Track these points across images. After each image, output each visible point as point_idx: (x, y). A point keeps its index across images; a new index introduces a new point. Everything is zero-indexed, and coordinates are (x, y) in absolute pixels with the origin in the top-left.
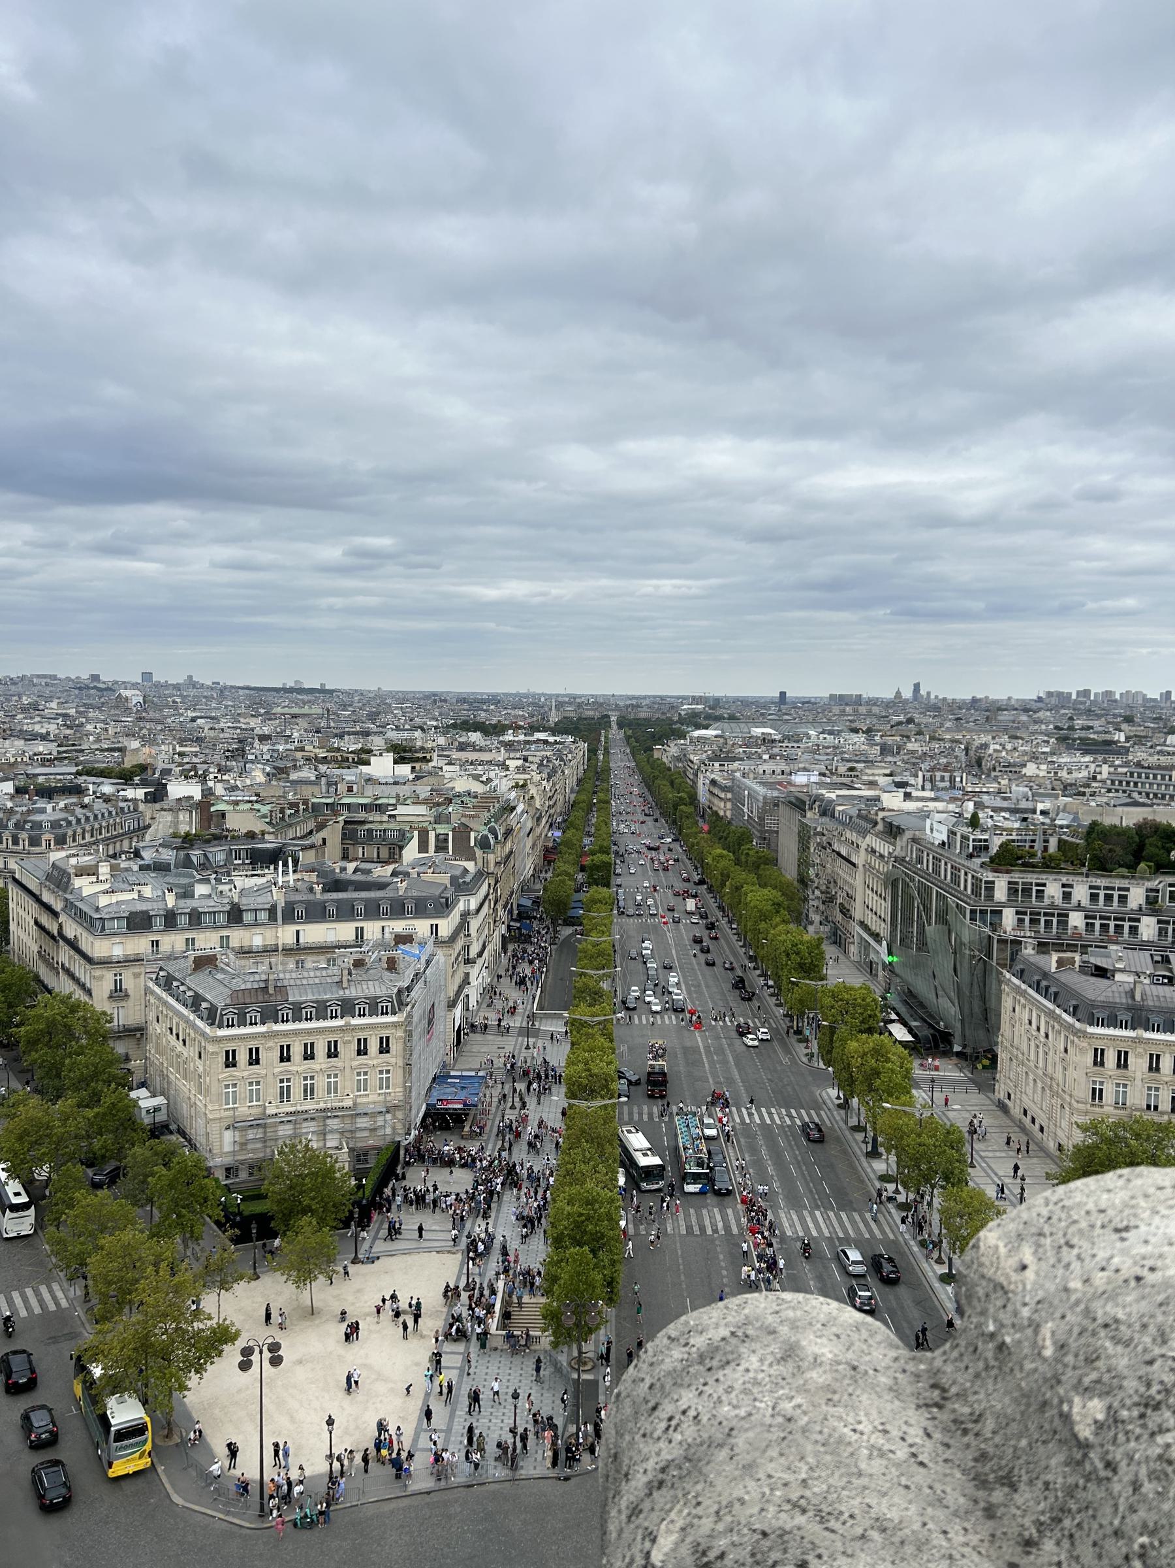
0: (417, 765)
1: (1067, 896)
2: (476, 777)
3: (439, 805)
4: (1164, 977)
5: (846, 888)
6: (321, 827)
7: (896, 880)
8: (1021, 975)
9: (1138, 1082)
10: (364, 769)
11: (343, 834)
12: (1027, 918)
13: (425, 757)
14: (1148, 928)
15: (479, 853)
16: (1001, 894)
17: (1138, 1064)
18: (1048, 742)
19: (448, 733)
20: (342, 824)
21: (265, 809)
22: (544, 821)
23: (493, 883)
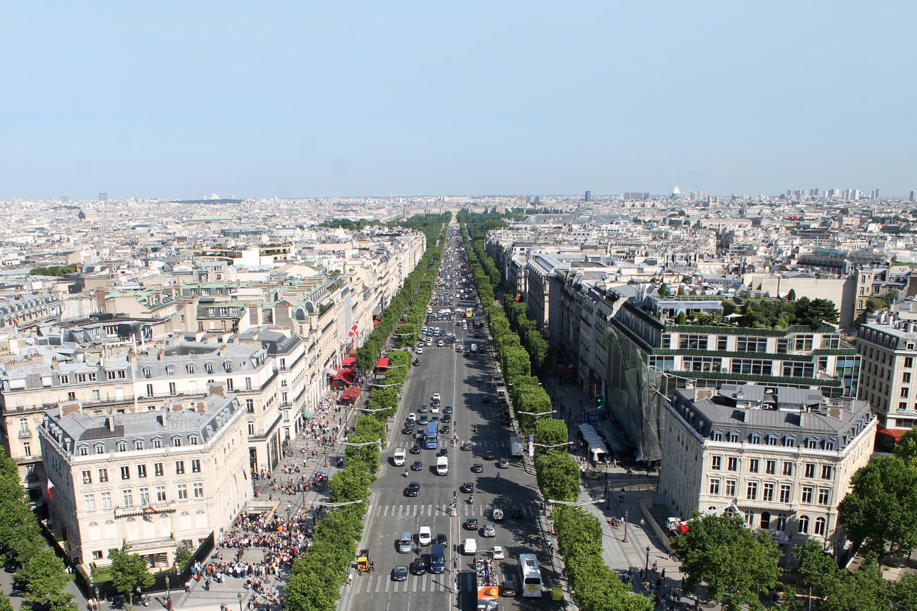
0: (278, 256)
1: (722, 345)
2: (309, 264)
4: (770, 404)
5: (585, 343)
10: (236, 261)
11: (199, 312)
12: (692, 363)
13: (284, 250)
15: (296, 323)
16: (674, 344)
19: (321, 229)
20: (196, 303)
21: (144, 295)
22: (373, 296)
23: (308, 345)
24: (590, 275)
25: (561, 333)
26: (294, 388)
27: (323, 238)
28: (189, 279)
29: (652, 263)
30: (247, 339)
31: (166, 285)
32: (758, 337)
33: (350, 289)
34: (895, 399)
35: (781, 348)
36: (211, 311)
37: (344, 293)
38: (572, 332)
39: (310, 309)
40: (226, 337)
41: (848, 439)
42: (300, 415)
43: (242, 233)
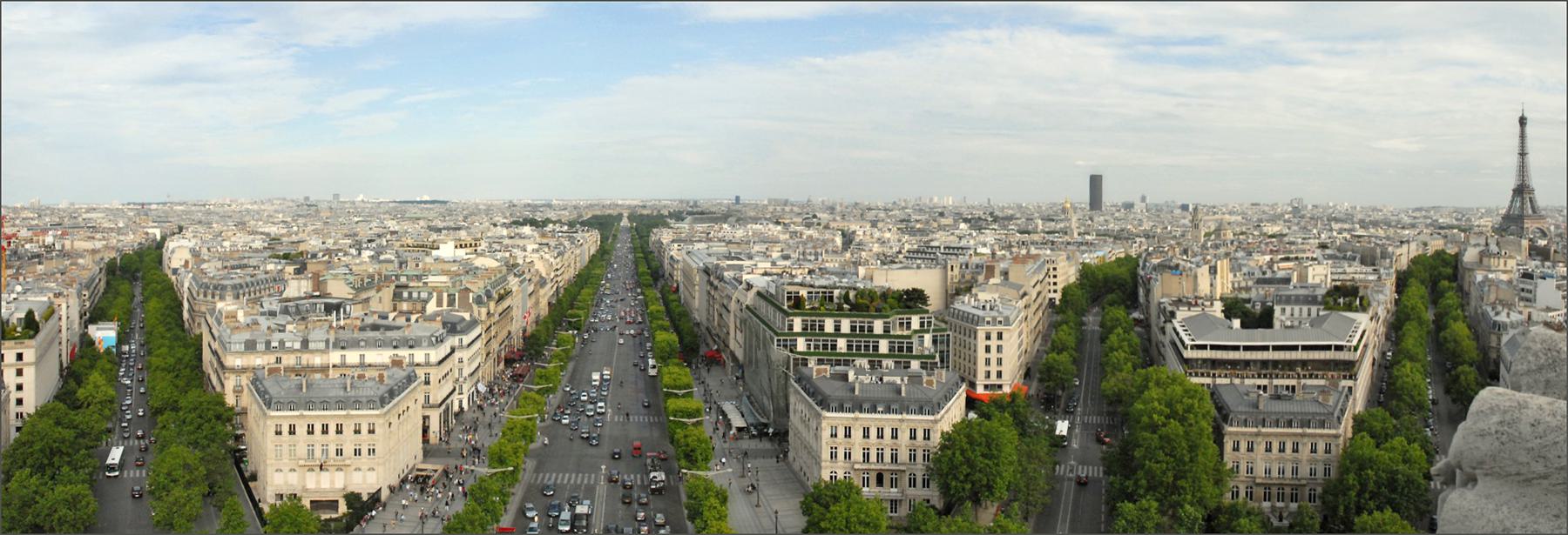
1: (837, 328)
3: (459, 275)
6: (379, 290)
7: (746, 320)
8: (798, 381)
9: (857, 446)
10: (435, 253)
11: (395, 294)
12: (812, 343)
14: (884, 346)
15: (475, 307)
16: (797, 328)
17: (857, 434)
18: (890, 230)
20: (393, 287)
21: (351, 278)
22: (549, 285)
24: (730, 267)
25: (708, 319)
26: (469, 364)
27: (513, 235)
28: (390, 267)
29: (786, 258)
30: (432, 318)
31: (371, 270)
32: (866, 320)
33: (528, 278)
34: (981, 369)
35: (887, 330)
36: (405, 295)
37: (522, 282)
38: (716, 318)
39: (489, 297)
40: (414, 318)
41: (942, 405)
42: (473, 389)
43: (444, 229)
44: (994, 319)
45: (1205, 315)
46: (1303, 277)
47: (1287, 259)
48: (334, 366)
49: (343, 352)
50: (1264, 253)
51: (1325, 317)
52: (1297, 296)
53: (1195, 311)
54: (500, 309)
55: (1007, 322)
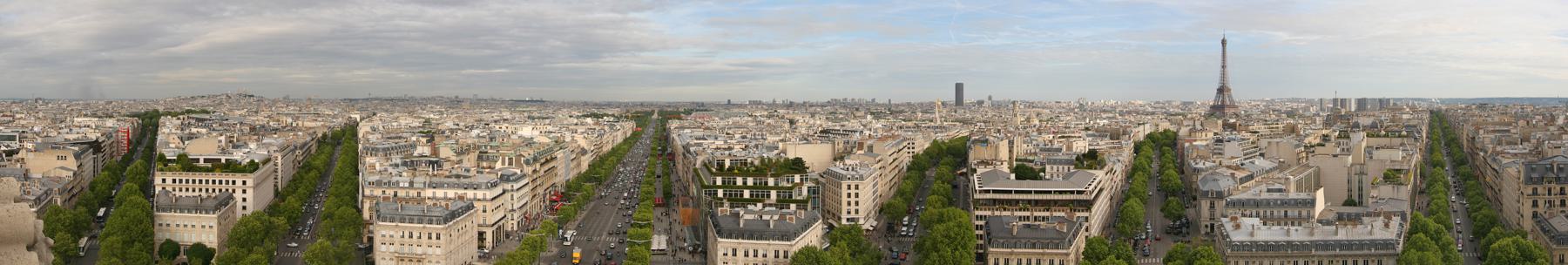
15: (525, 166)
20: (477, 152)
34: (845, 207)
35: (776, 184)
44: (853, 176)
45: (995, 171)
46: (1069, 148)
47: (1063, 137)
48: (429, 198)
49: (434, 190)
50: (1049, 133)
51: (1074, 173)
52: (1061, 160)
53: (990, 168)
54: (546, 168)
55: (862, 178)
